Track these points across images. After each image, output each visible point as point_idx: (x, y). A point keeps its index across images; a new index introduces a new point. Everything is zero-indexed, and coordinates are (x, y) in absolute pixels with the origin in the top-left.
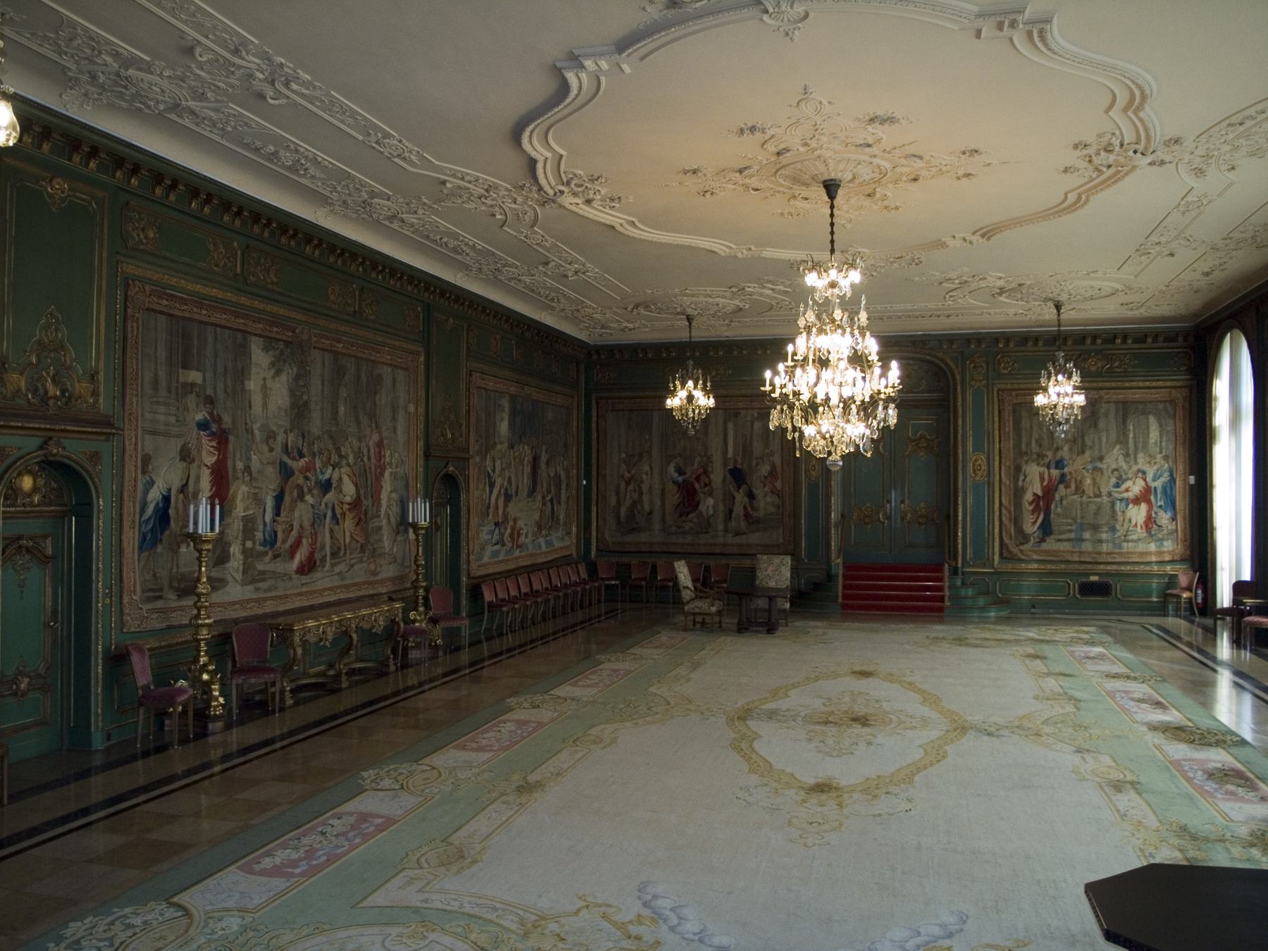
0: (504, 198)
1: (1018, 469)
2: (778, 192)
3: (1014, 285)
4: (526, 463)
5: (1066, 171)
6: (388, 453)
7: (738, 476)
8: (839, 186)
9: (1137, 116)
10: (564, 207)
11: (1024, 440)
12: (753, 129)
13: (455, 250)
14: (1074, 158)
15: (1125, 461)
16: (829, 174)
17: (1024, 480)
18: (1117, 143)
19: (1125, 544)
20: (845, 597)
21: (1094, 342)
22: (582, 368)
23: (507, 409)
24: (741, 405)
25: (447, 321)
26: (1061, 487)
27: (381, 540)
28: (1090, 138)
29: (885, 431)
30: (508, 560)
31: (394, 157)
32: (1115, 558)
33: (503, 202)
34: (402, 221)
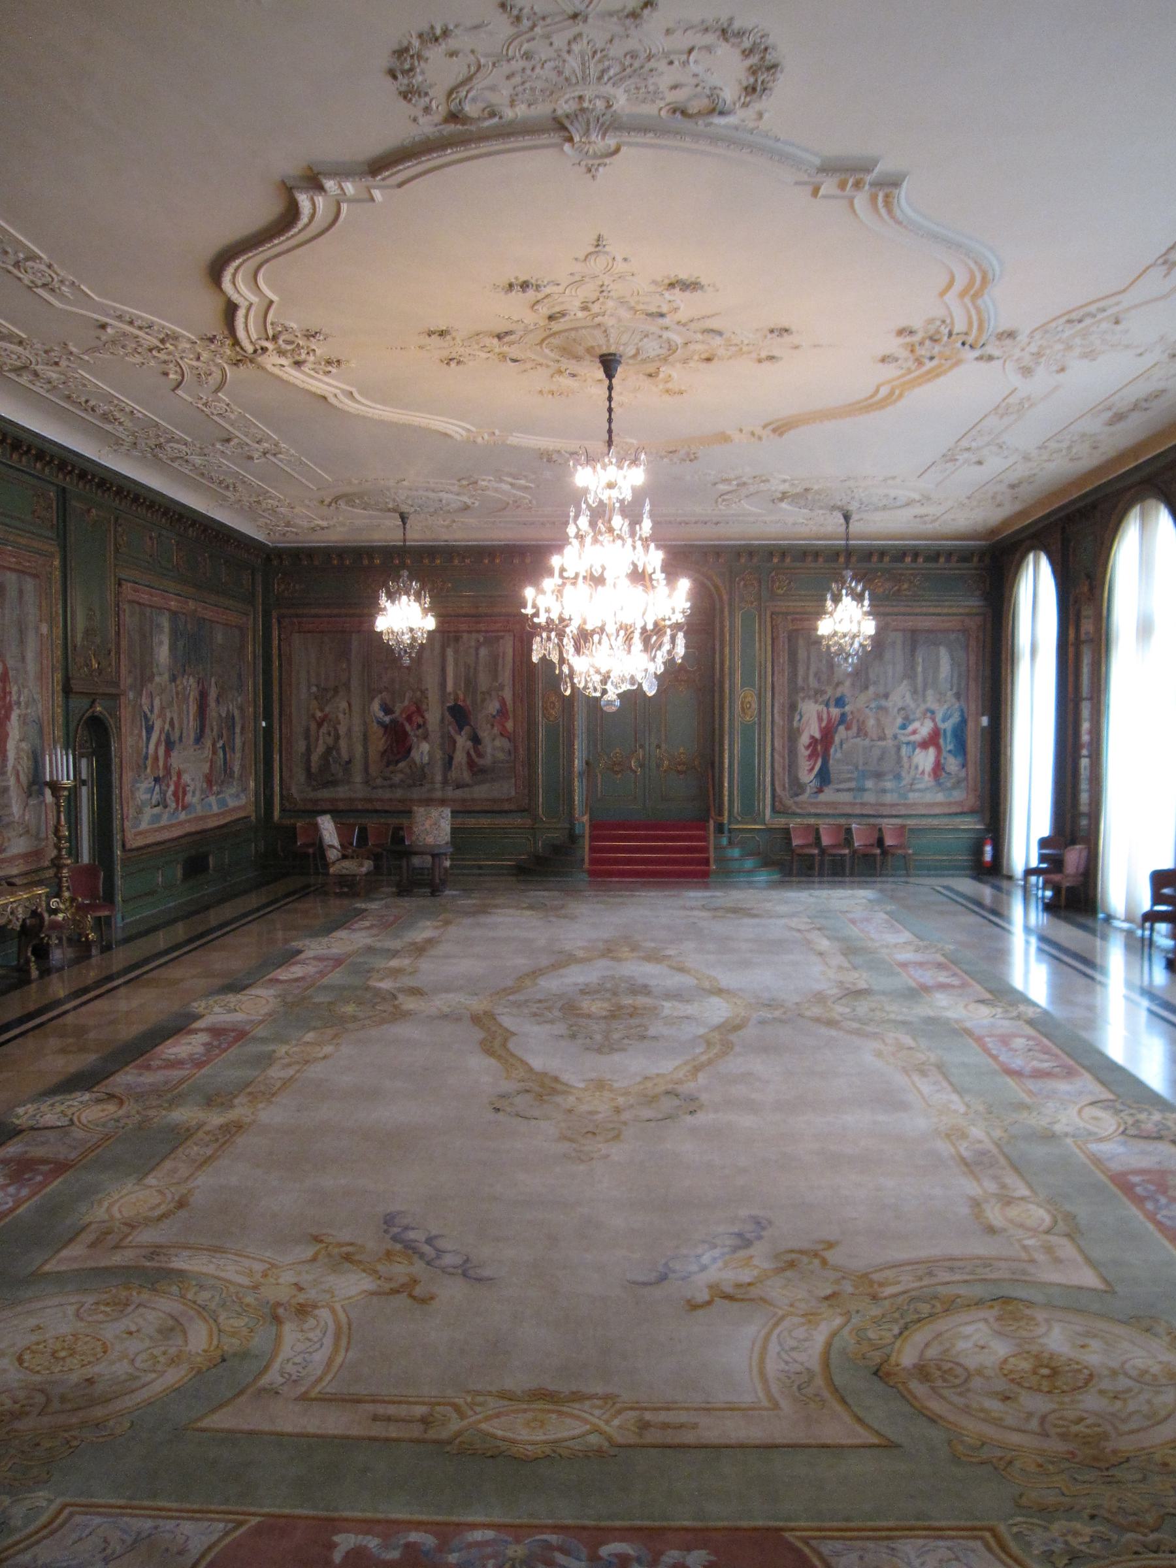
0: (184, 352)
1: (793, 707)
2: (541, 365)
3: (799, 490)
4: (191, 699)
5: (883, 360)
6: (15, 689)
7: (459, 715)
8: (619, 362)
9: (973, 303)
10: (264, 369)
12: (525, 286)
13: (105, 417)
14: (894, 345)
16: (608, 347)
18: (946, 331)
19: (911, 795)
20: (593, 861)
22: (259, 578)
23: (167, 630)
24: (464, 627)
25: (89, 511)
27: (8, 806)
28: (917, 323)
29: (670, 663)
30: (172, 826)
31: (37, 287)
33: (181, 358)
34: (36, 374)
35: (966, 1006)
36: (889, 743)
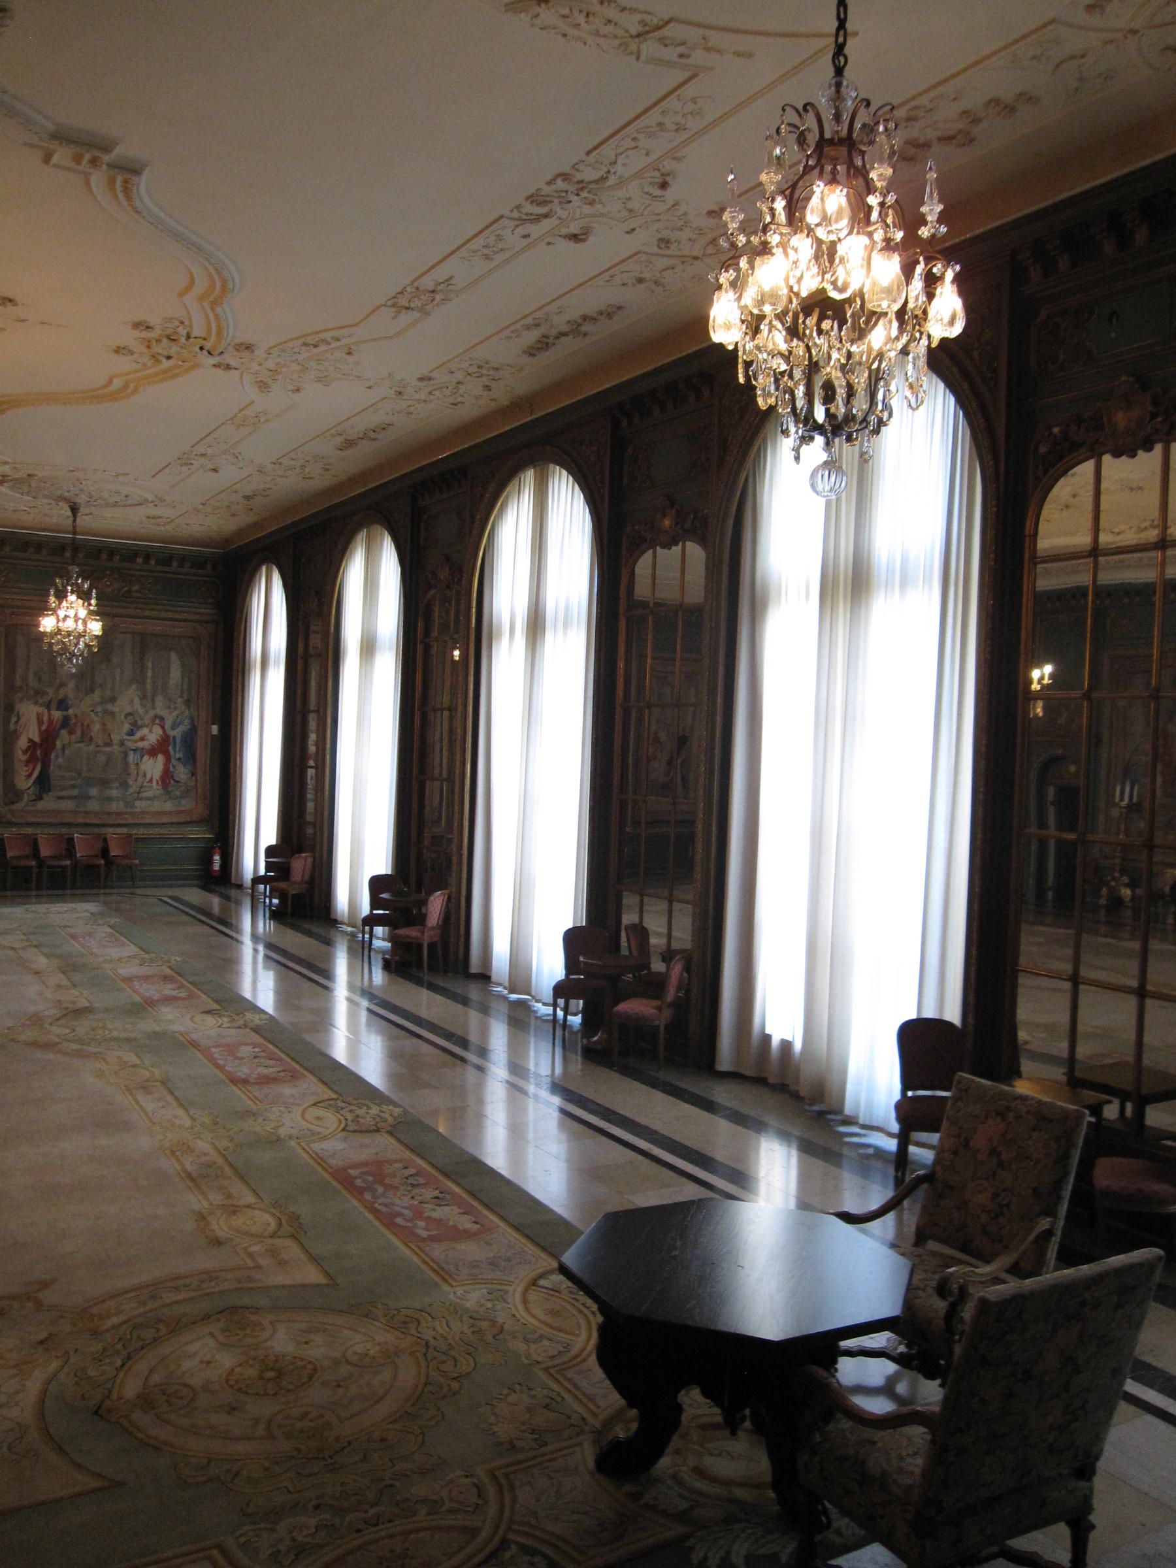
3: (21, 474)
5: (118, 350)
9: (213, 309)
11: (20, 671)
14: (129, 337)
15: (141, 704)
17: (17, 722)
19: (138, 803)
21: (110, 558)
26: (64, 732)
28: (154, 320)
32: (126, 819)
35: (192, 1019)
36: (116, 748)
